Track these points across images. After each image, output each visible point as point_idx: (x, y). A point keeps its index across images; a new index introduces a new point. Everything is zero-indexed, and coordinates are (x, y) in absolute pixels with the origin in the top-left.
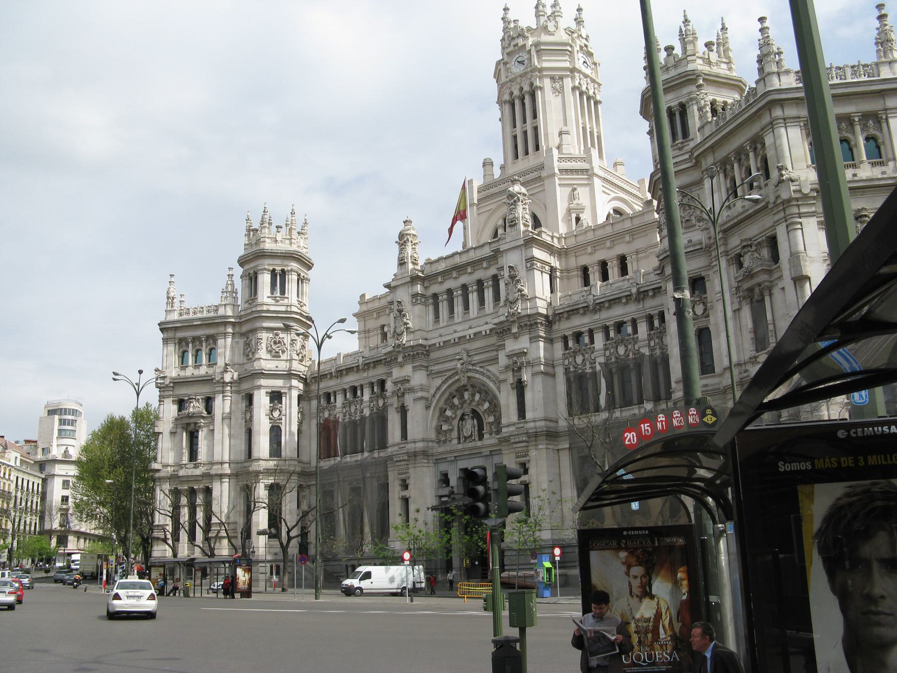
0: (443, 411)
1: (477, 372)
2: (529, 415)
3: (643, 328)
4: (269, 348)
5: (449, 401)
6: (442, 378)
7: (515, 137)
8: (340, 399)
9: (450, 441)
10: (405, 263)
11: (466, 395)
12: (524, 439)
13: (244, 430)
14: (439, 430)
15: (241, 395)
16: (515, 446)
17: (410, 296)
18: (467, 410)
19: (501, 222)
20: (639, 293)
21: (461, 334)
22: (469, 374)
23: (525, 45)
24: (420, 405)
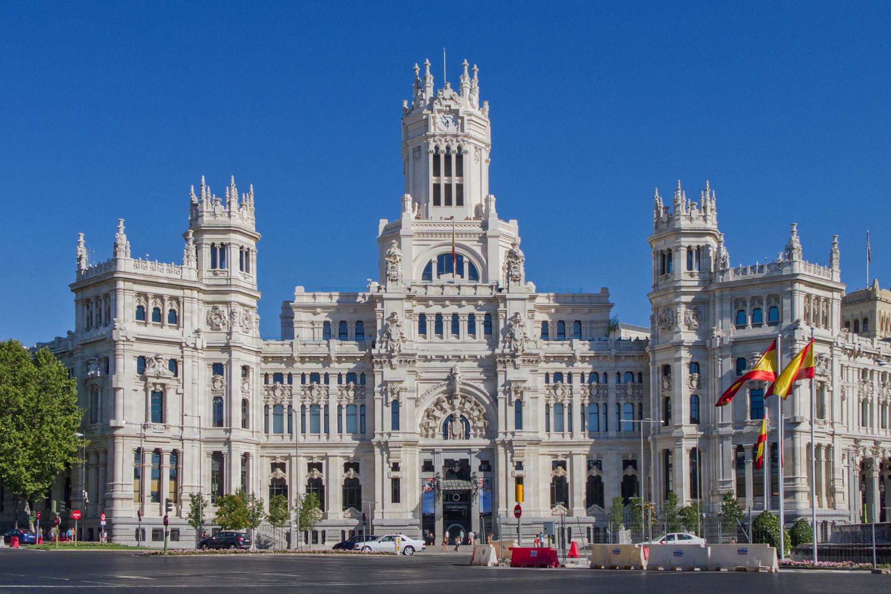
0: (429, 414)
1: (469, 385)
2: (525, 427)
3: (612, 381)
4: (242, 324)
7: (437, 187)
8: (297, 381)
9: (433, 436)
10: (397, 280)
11: (457, 403)
12: (525, 444)
14: (426, 427)
15: (207, 362)
17: (404, 311)
18: (458, 415)
19: (435, 259)
22: (463, 387)
23: (458, 110)
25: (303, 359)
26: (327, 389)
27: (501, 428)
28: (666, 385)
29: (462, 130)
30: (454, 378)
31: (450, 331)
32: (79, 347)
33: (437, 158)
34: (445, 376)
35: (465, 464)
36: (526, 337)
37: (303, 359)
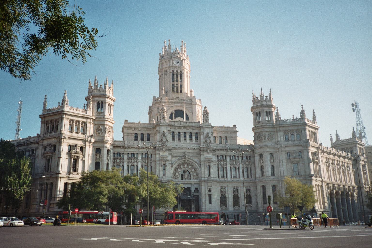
0: (176, 170)
1: (191, 159)
2: (212, 176)
5: (179, 165)
6: (177, 159)
7: (173, 85)
8: (126, 157)
9: (178, 178)
11: (186, 166)
13: (95, 162)
14: (174, 174)
16: (208, 183)
18: (187, 170)
19: (174, 112)
20: (242, 150)
21: (185, 147)
22: (188, 160)
24: (170, 166)
25: (128, 147)
26: (137, 159)
27: (203, 176)
28: (261, 161)
29: (182, 66)
30: (185, 156)
31: (183, 139)
32: (42, 140)
33: (173, 75)
34: (181, 155)
35: (189, 189)
36: (211, 142)
37: (128, 147)
